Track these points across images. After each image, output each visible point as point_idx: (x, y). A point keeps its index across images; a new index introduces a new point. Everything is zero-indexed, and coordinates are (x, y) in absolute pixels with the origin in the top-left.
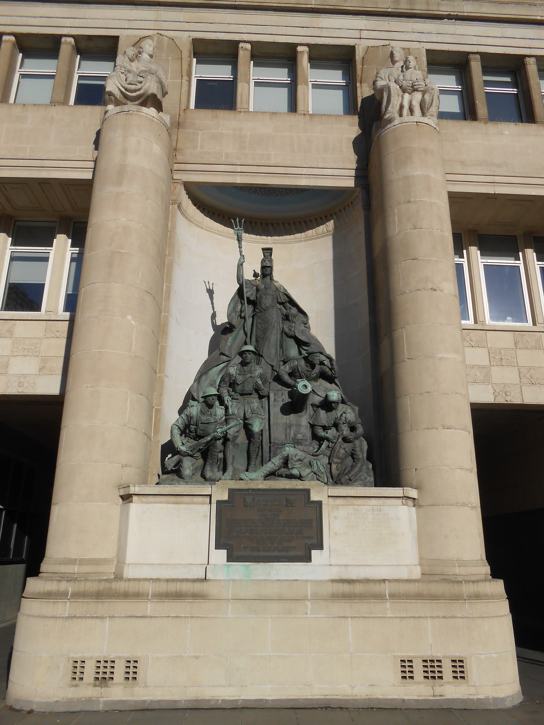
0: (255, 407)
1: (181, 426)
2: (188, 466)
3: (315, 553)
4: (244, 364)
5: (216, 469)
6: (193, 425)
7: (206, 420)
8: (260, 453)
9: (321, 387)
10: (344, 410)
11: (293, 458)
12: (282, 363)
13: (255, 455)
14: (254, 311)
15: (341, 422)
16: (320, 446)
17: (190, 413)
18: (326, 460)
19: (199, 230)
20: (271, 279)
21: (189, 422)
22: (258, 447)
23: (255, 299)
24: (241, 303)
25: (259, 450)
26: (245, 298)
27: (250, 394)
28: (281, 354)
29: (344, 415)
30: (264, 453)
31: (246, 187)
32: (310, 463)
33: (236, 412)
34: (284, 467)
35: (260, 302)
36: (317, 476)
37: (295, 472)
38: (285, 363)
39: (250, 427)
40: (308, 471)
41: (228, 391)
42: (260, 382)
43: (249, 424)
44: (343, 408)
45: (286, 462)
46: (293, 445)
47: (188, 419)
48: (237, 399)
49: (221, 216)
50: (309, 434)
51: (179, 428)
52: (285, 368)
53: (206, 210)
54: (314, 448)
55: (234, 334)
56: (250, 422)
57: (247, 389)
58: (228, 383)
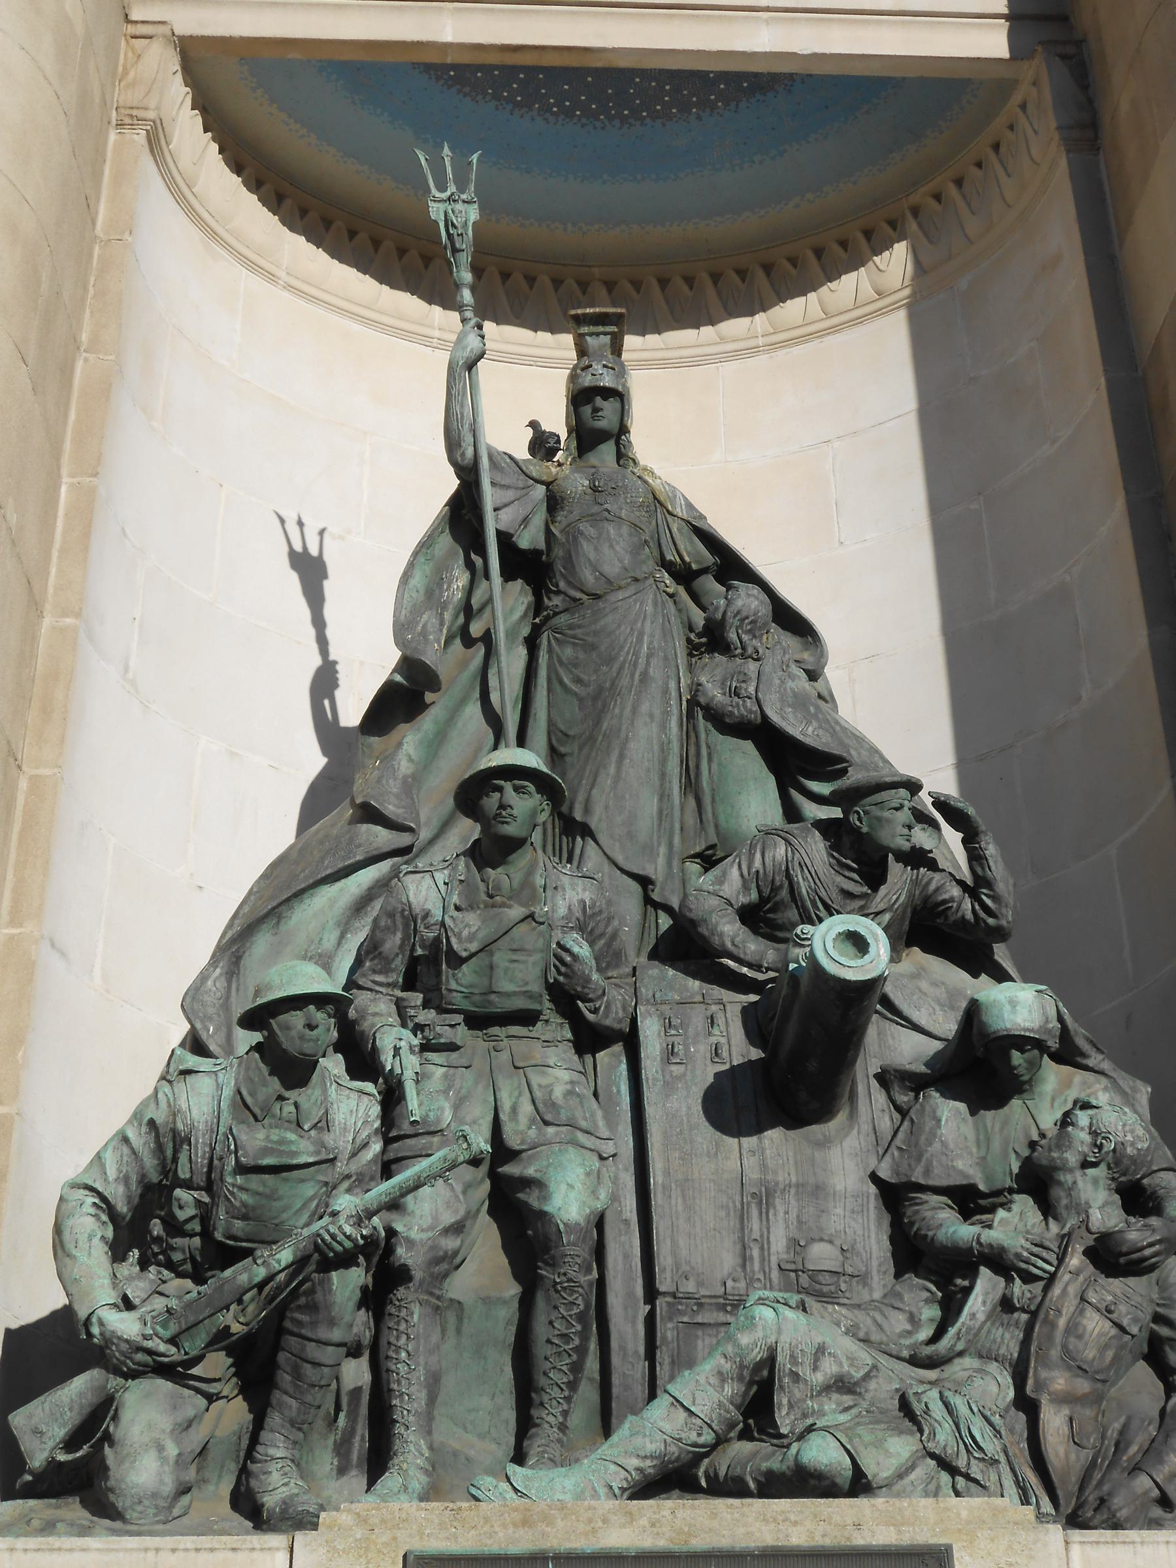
0: (558, 1092)
1: (118, 1195)
2: (151, 1433)
4: (492, 851)
5: (324, 1461)
6: (188, 1185)
7: (266, 1151)
8: (592, 1365)
9: (924, 985)
10: (1073, 1094)
11: (805, 1371)
12: (694, 867)
13: (564, 1363)
14: (538, 607)
15: (1072, 1159)
16: (951, 1307)
17: (174, 1113)
18: (997, 1387)
19: (256, 283)
20: (623, 456)
21: (168, 1168)
22: (582, 1317)
23: (542, 545)
24: (470, 565)
25: (584, 1337)
27: (528, 1018)
28: (691, 820)
29: (1083, 1118)
30: (616, 1360)
31: (487, 69)
32: (905, 1406)
33: (448, 1116)
34: (745, 1435)
35: (569, 561)
37: (822, 1453)
38: (708, 860)
39: (531, 1198)
40: (903, 1446)
41: (401, 1008)
42: (582, 949)
43: (527, 1183)
44: (1067, 1084)
46: (794, 1299)
47: (160, 1148)
48: (452, 1047)
49: (363, 237)
50: (873, 1240)
51: (105, 1204)
52: (721, 881)
53: (288, 203)
54: (913, 1319)
55: (428, 722)
56: (530, 1171)
57: (508, 987)
58: (400, 964)
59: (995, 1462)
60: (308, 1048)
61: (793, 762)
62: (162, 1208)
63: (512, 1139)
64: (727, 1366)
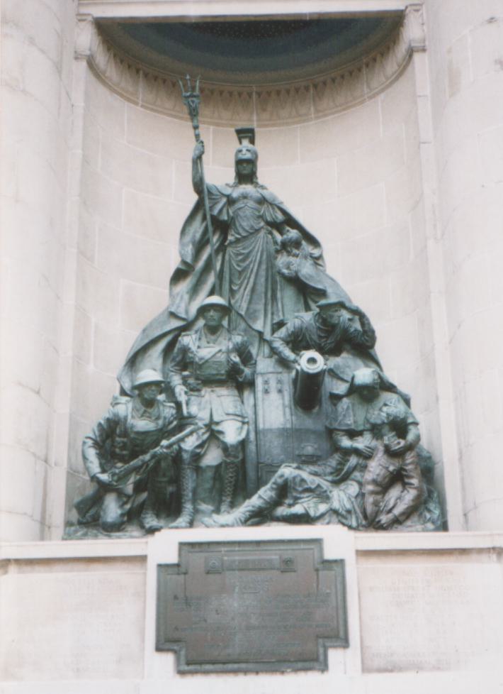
2: (112, 509)
3: (334, 655)
6: (120, 436)
26: (208, 217)
36: (339, 516)
39: (221, 437)
43: (221, 432)
45: (284, 491)
53: (141, 72)
59: (349, 512)
60: (152, 396)
61: (306, 292)
62: (113, 441)
63: (216, 419)
64: (274, 486)
